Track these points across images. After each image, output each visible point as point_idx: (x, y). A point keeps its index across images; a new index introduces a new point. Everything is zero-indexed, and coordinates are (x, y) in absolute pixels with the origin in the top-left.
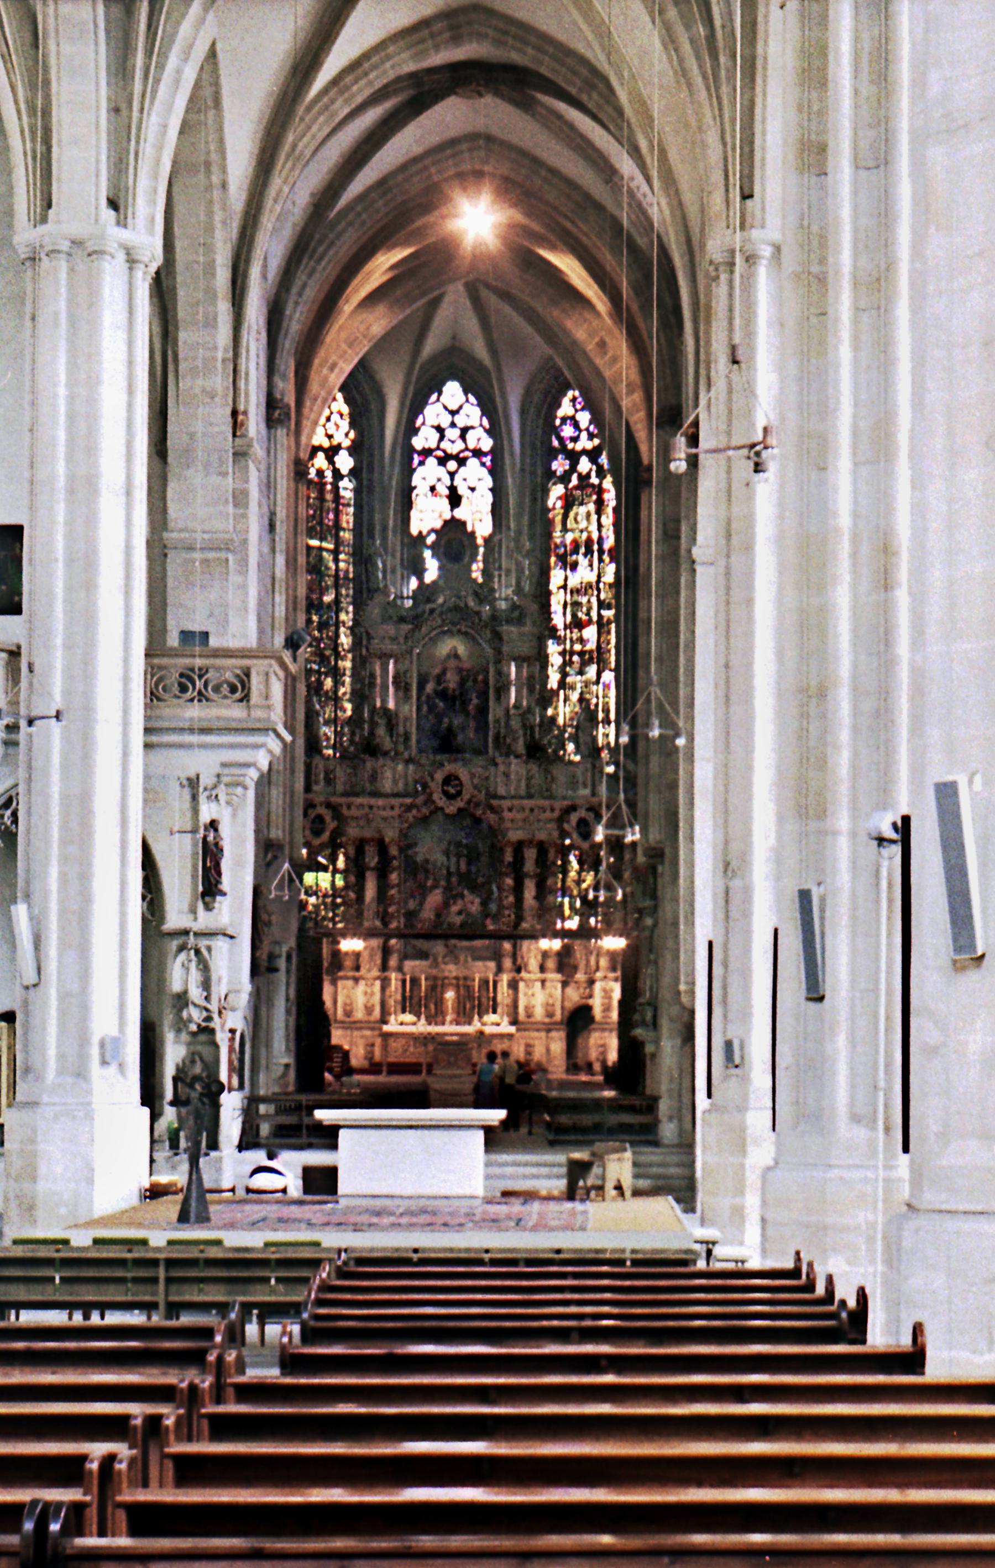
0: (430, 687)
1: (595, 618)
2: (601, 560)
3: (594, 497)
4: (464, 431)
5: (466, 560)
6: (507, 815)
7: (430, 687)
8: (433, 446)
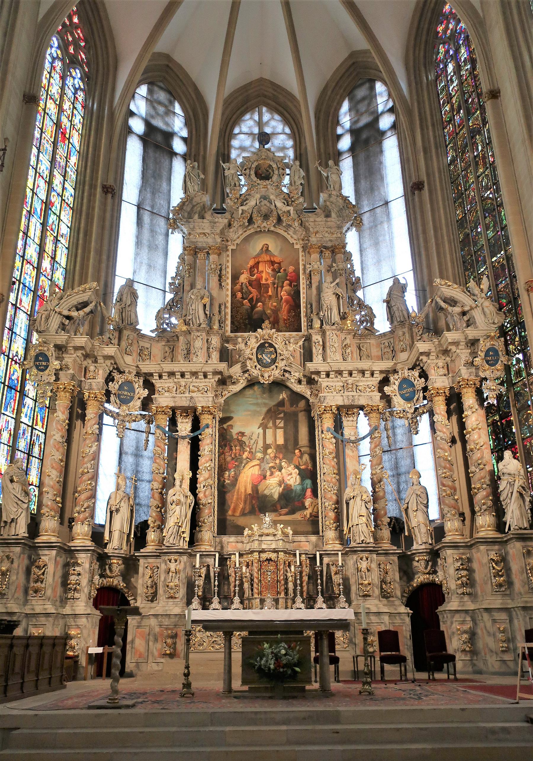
0: (243, 278)
5: (275, 178)
6: (323, 382)
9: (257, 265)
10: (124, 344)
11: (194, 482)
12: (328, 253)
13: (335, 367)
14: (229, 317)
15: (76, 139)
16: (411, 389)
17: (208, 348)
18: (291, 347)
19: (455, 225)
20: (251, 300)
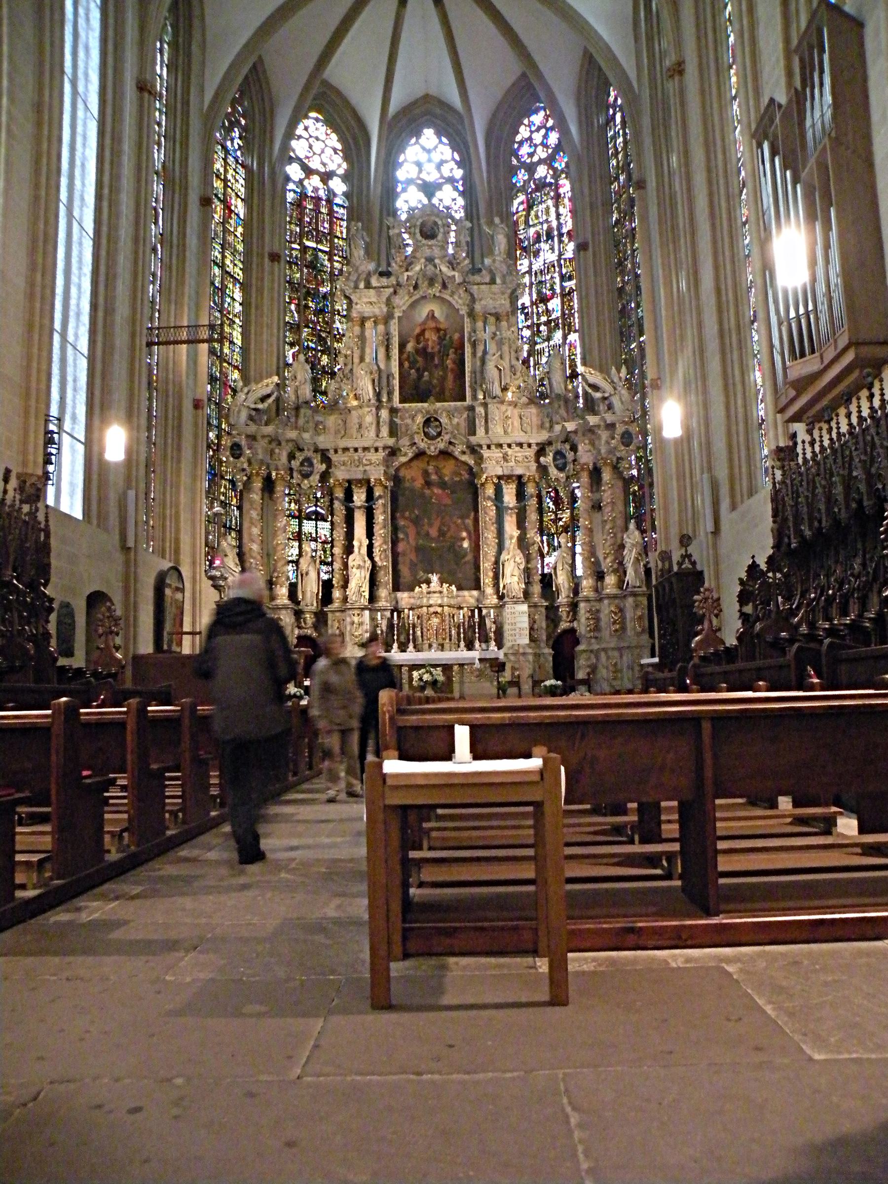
0: (410, 347)
1: (558, 291)
2: (561, 242)
3: (552, 194)
6: (486, 453)
8: (414, 176)
9: (423, 332)
10: (301, 421)
11: (370, 547)
12: (492, 319)
13: (495, 441)
14: (397, 388)
15: (240, 208)
17: (378, 423)
18: (455, 421)
19: (616, 294)
20: (418, 370)
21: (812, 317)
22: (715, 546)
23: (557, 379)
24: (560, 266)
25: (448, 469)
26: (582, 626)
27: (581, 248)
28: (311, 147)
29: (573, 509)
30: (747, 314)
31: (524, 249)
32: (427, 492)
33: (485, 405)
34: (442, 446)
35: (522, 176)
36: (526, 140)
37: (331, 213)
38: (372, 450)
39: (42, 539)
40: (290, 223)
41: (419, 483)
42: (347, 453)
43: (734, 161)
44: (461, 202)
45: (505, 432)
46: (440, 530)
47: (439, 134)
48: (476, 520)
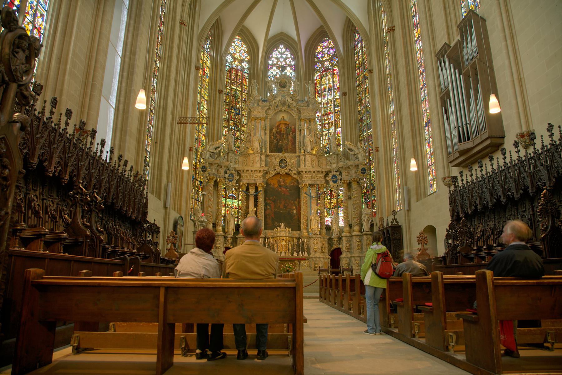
0: (274, 130)
1: (333, 111)
2: (334, 92)
4: (285, 60)
5: (287, 87)
6: (304, 175)
7: (274, 130)
8: (275, 63)
9: (279, 125)
12: (308, 121)
14: (268, 147)
15: (208, 71)
16: (336, 179)
17: (261, 161)
18: (292, 161)
19: (358, 113)
20: (277, 140)
21: (468, 126)
22: (409, 216)
23: (333, 146)
24: (334, 101)
25: (288, 181)
26: (344, 247)
27: (344, 94)
28: (236, 49)
29: (338, 199)
30: (422, 124)
31: (319, 94)
32: (279, 189)
33: (304, 155)
34: (287, 171)
35: (319, 65)
36: (321, 52)
37: (242, 75)
38: (258, 171)
39: (145, 201)
40: (226, 78)
41: (276, 185)
42: (248, 172)
43: (416, 65)
44: (294, 74)
45: (312, 166)
46: (284, 205)
47: (286, 47)
48: (299, 202)
